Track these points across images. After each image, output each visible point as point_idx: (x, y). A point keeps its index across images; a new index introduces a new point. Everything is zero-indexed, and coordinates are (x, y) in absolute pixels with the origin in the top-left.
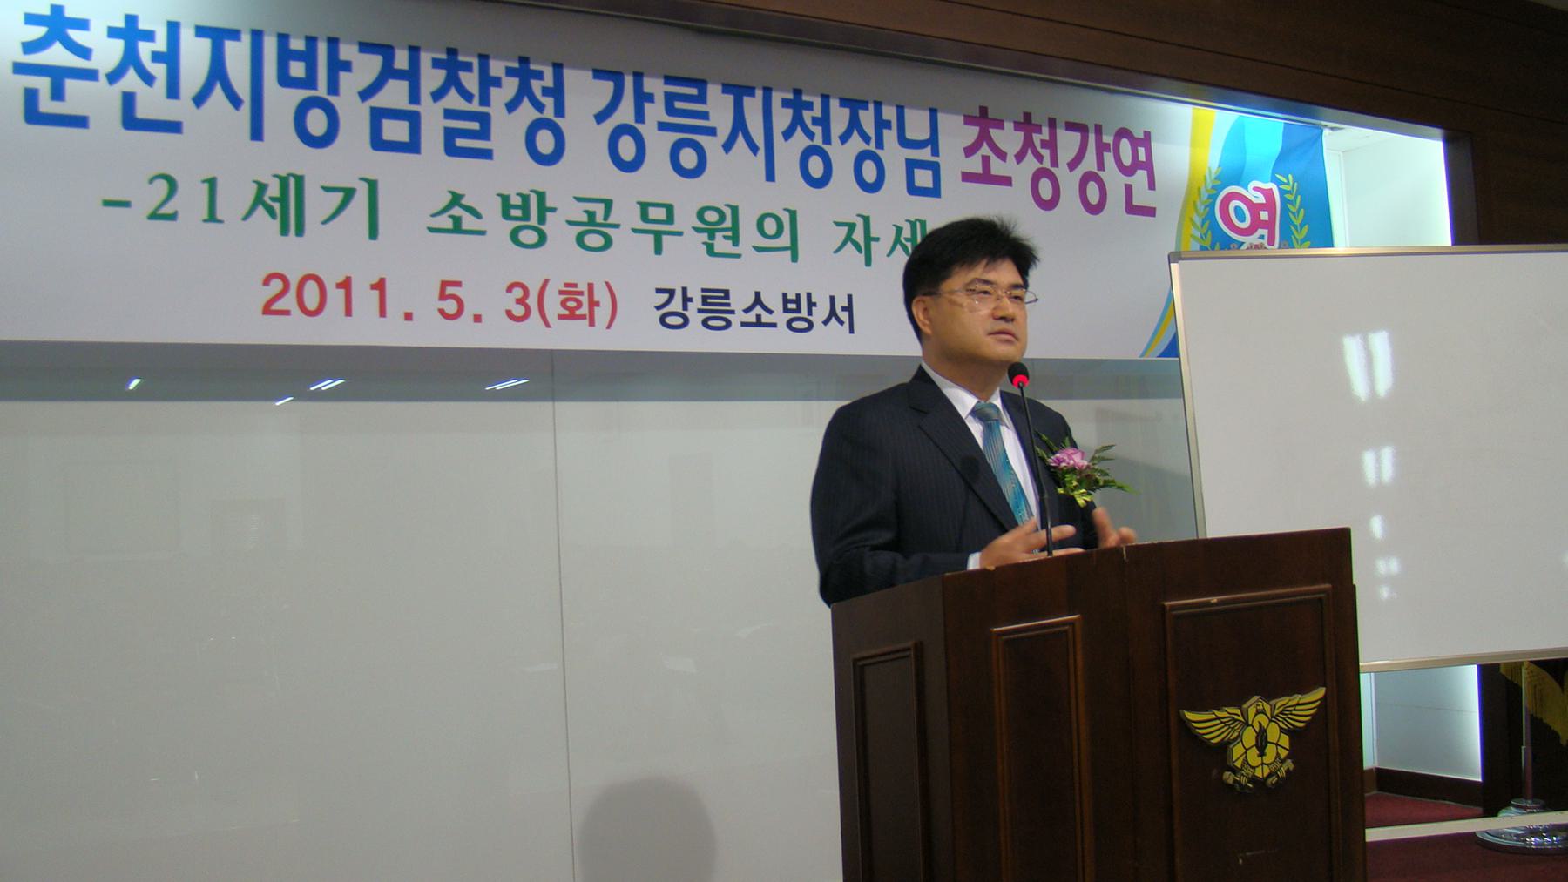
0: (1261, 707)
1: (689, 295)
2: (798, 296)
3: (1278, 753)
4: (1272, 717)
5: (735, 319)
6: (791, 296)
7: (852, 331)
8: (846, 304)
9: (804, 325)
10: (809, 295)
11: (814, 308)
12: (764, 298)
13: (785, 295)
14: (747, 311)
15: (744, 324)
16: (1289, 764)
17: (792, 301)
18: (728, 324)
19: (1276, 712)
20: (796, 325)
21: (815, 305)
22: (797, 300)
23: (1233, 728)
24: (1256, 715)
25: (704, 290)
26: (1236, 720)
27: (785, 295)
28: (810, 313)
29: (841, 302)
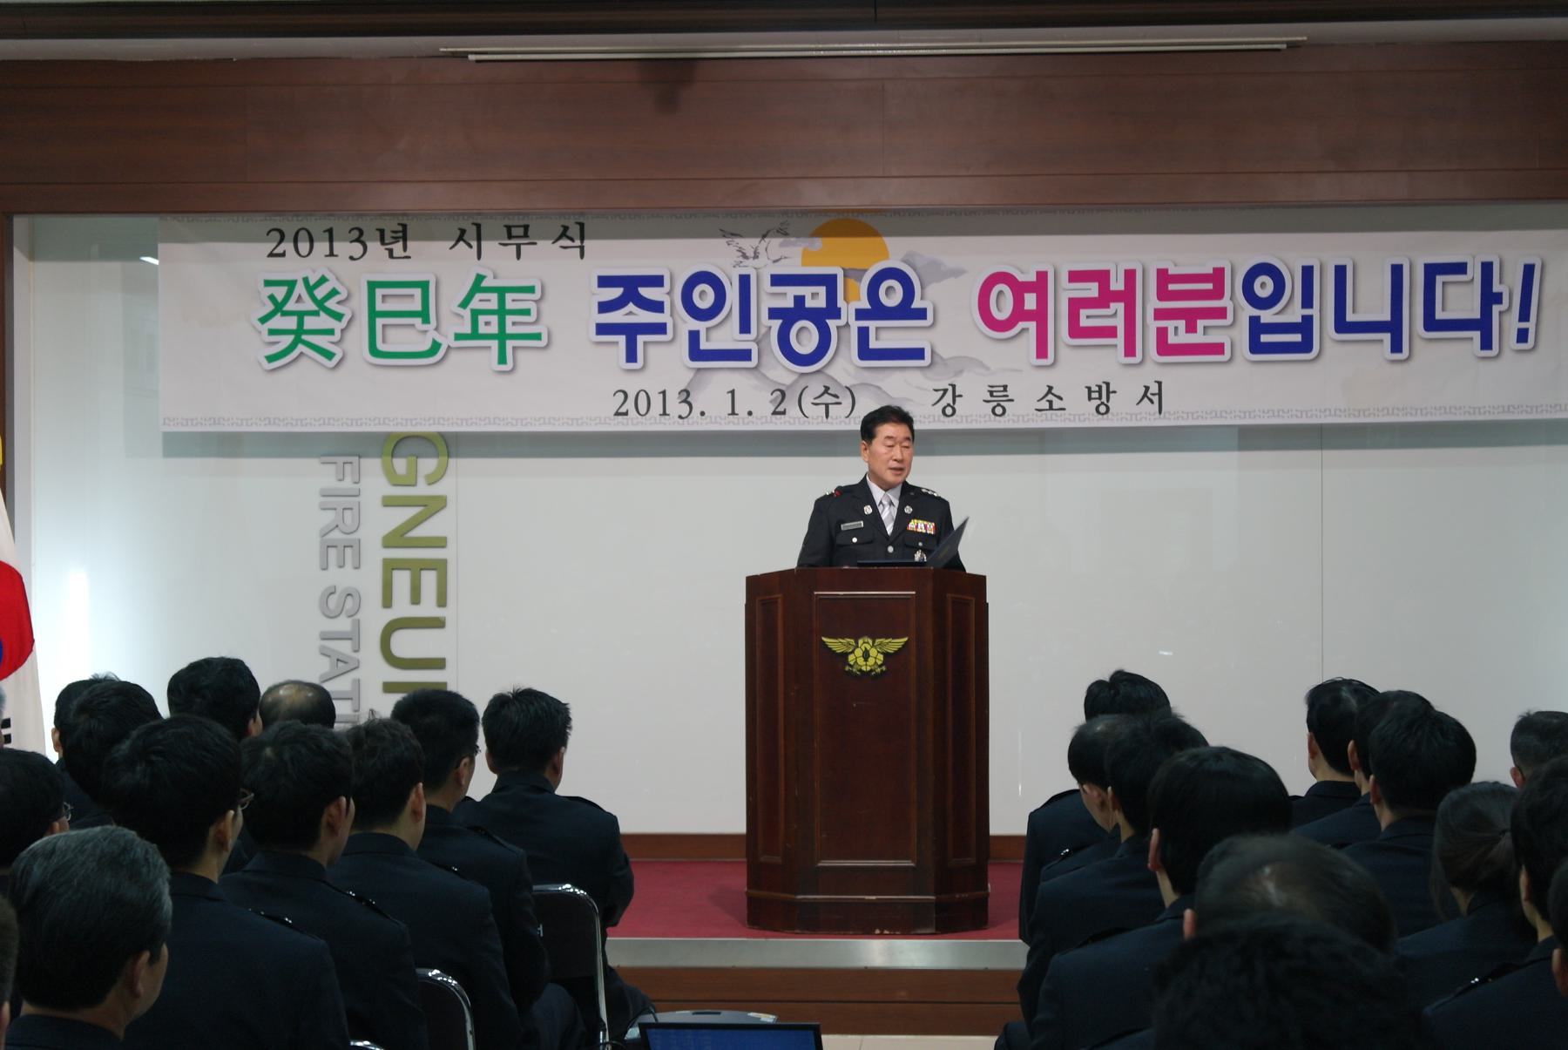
16: (884, 668)
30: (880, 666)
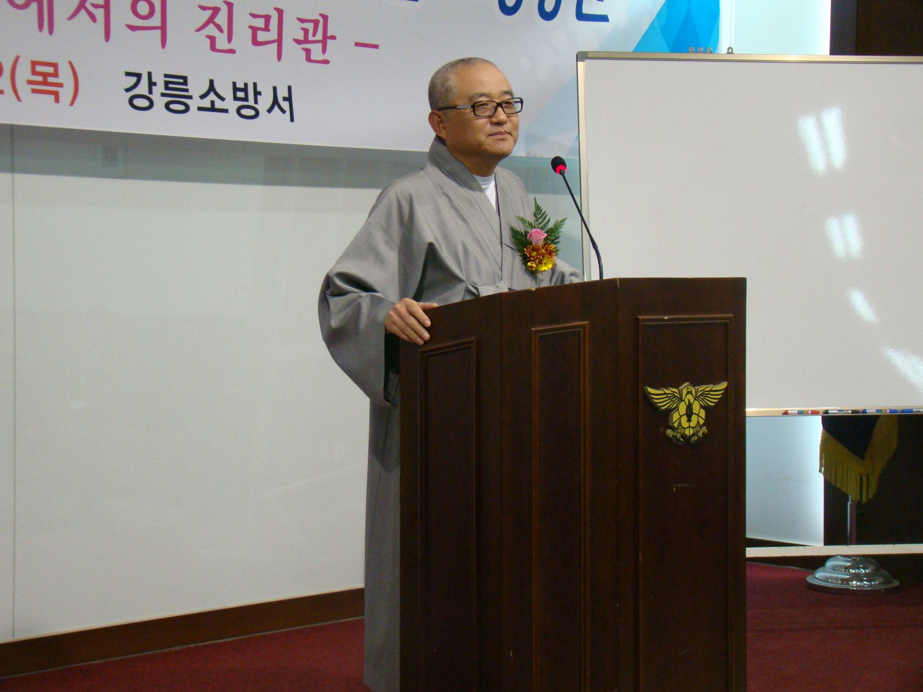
0: (690, 390)
1: (154, 80)
2: (246, 85)
3: (698, 421)
4: (696, 397)
5: (194, 104)
6: (240, 85)
7: (292, 120)
8: (287, 95)
9: (252, 113)
10: (255, 85)
11: (259, 97)
12: (217, 86)
13: (234, 84)
14: (203, 97)
15: (200, 109)
16: (705, 429)
17: (240, 90)
18: (187, 108)
19: (698, 394)
20: (245, 112)
21: (260, 93)
22: (245, 90)
23: (674, 401)
24: (687, 395)
25: (166, 76)
26: (675, 396)
27: (234, 84)
28: (256, 102)
29: (282, 93)
30: (701, 427)
